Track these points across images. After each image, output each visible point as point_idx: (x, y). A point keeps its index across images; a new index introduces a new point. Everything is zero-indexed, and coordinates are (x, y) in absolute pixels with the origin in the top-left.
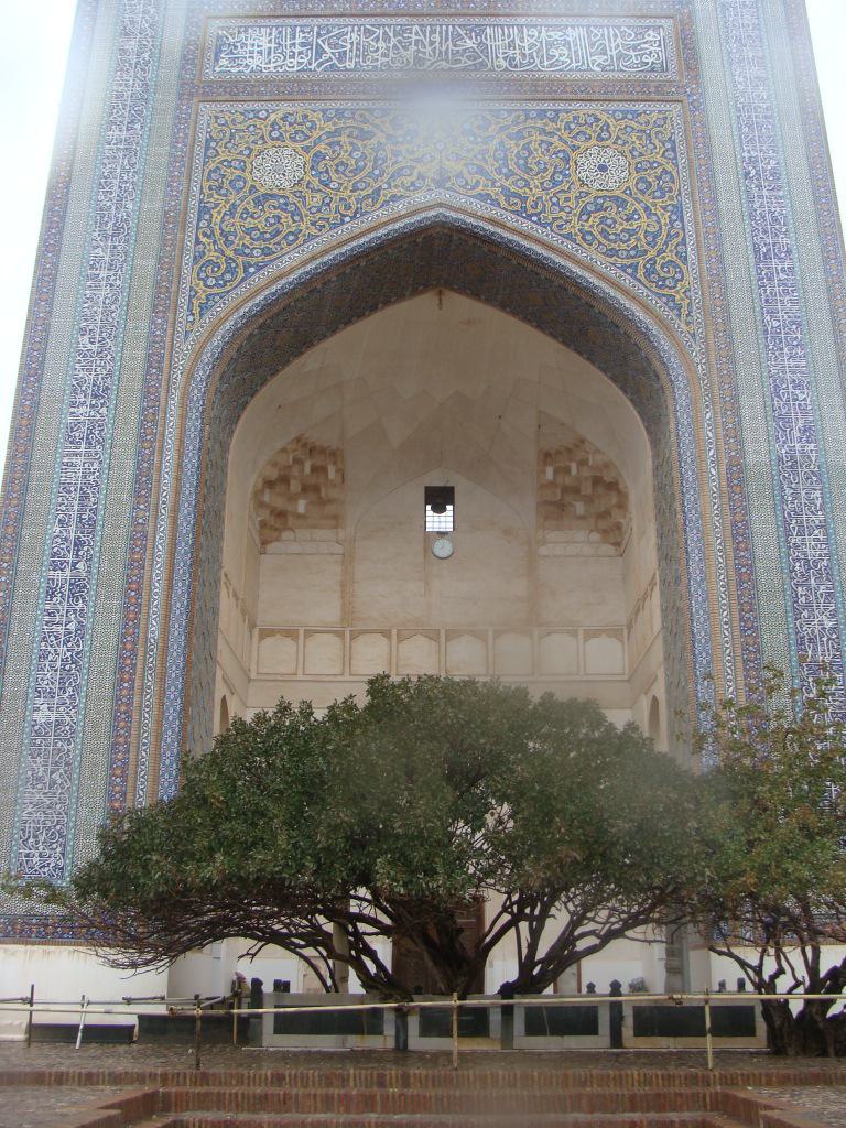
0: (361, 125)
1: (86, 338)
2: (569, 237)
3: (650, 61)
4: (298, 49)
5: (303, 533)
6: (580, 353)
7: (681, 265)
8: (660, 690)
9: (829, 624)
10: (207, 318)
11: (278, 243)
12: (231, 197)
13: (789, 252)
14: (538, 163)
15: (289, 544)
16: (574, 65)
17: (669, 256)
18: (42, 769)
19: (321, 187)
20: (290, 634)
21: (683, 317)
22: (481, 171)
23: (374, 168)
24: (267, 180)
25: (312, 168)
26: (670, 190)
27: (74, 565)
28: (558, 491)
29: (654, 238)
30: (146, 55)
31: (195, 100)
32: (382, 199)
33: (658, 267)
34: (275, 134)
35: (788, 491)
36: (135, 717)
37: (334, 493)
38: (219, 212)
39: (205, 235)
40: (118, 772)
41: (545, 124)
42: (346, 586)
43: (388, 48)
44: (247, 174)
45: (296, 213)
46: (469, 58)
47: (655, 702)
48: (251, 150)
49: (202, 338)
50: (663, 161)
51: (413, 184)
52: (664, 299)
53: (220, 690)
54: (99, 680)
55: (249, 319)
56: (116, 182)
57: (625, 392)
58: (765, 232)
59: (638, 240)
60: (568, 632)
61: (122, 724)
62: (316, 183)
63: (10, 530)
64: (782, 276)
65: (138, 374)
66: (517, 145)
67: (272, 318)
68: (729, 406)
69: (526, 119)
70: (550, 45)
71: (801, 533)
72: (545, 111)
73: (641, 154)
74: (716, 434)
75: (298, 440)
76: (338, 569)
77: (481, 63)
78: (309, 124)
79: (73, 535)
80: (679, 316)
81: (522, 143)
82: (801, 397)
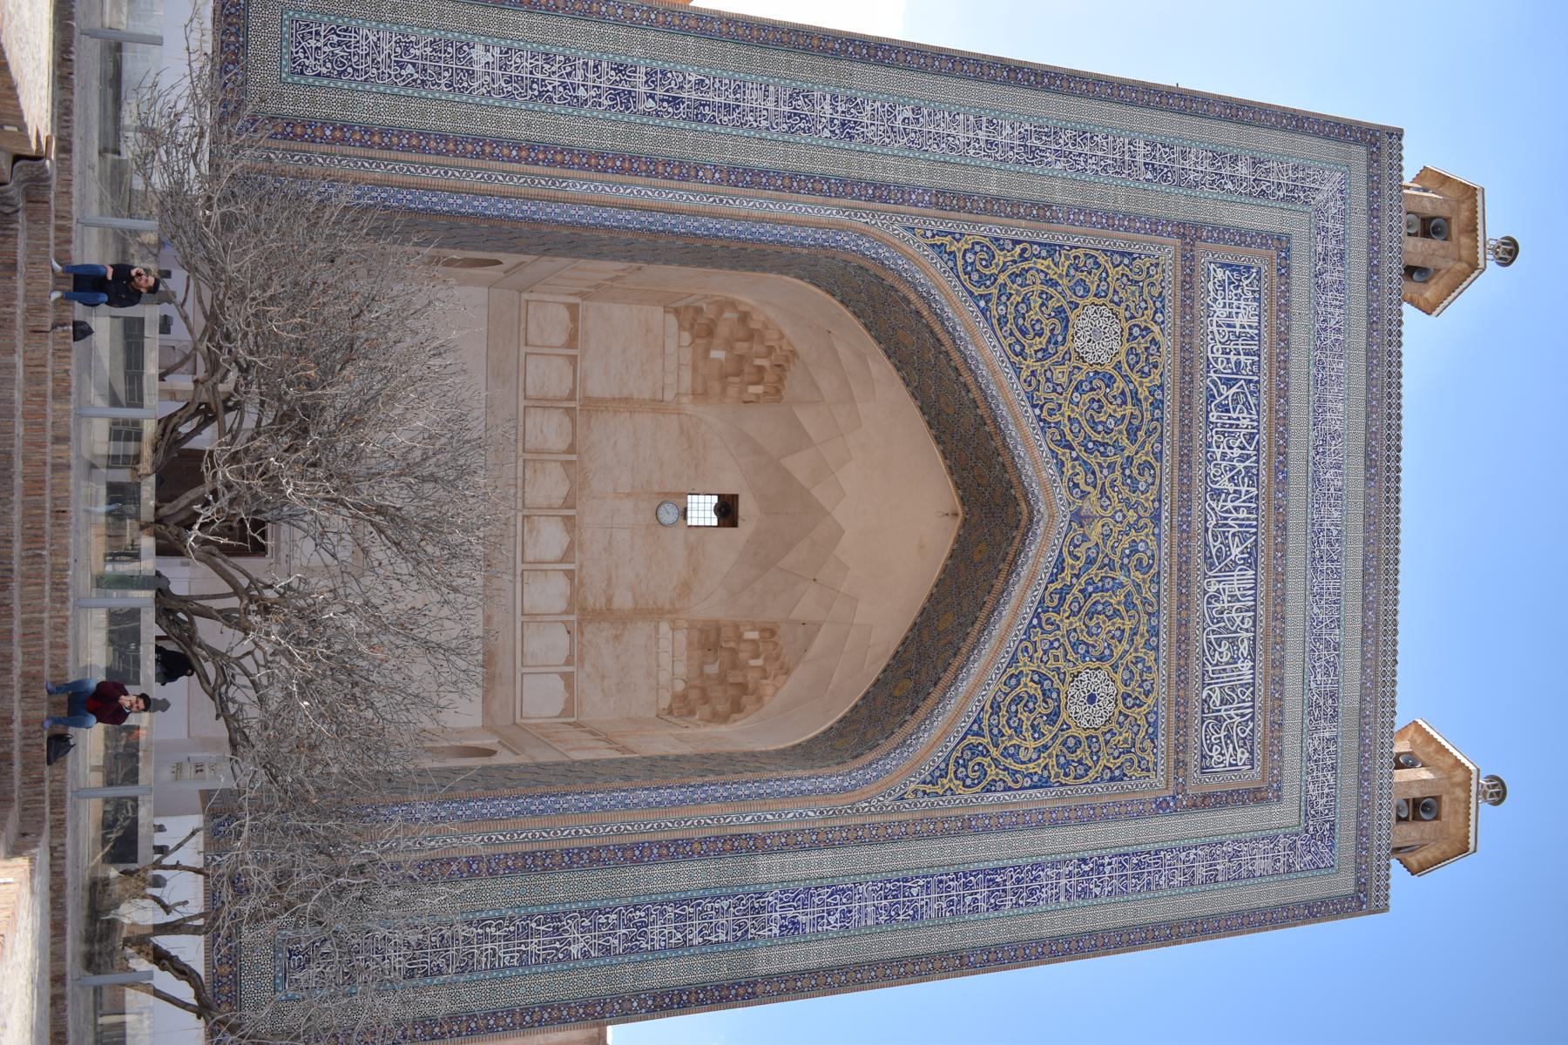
0: (1144, 428)
1: (910, 114)
2: (1014, 660)
3: (1214, 754)
4: (1233, 358)
5: (687, 356)
6: (885, 671)
7: (984, 783)
8: (504, 758)
9: (574, 949)
10: (929, 252)
11: (1012, 334)
12: (1065, 281)
13: (996, 907)
14: (1098, 626)
15: (677, 340)
16: (1210, 668)
17: (992, 772)
18: (418, 53)
19: (1074, 383)
20: (572, 341)
21: (922, 787)
22: (1090, 562)
23: (1095, 442)
24: (1082, 322)
25: (1096, 373)
26: (1066, 775)
27: (652, 96)
28: (732, 645)
29: (1011, 756)
30: (1230, 186)
31: (1178, 242)
32: (1060, 451)
33: (979, 759)
34: (1136, 331)
35: (725, 904)
36: (477, 163)
37: (732, 391)
38: (1048, 267)
39: (1024, 250)
40: (414, 142)
41: (1142, 635)
42: (626, 403)
43: (1231, 460)
44: (1091, 299)
46: (1220, 550)
47: (489, 753)
48: (1118, 304)
49: (902, 244)
50: (1099, 767)
51: (1076, 485)
52: (943, 766)
53: (509, 259)
54: (521, 122)
55: (927, 300)
56: (1086, 150)
57: (840, 721)
58: (1018, 881)
59: (1011, 738)
60: (571, 655)
61: (470, 147)
62: (1079, 376)
63: (693, 23)
64: (968, 900)
65: (867, 174)
66: (1119, 603)
67: (927, 326)
68: (822, 837)
69: (1149, 614)
70: (1233, 642)
71: (678, 917)
72: (1157, 635)
73: (1107, 742)
74: (790, 821)
75: (794, 353)
76: (647, 396)
77: (1212, 564)
78: (1146, 369)
79: (686, 95)
80: (924, 782)
81: (1122, 608)
82: (832, 919)
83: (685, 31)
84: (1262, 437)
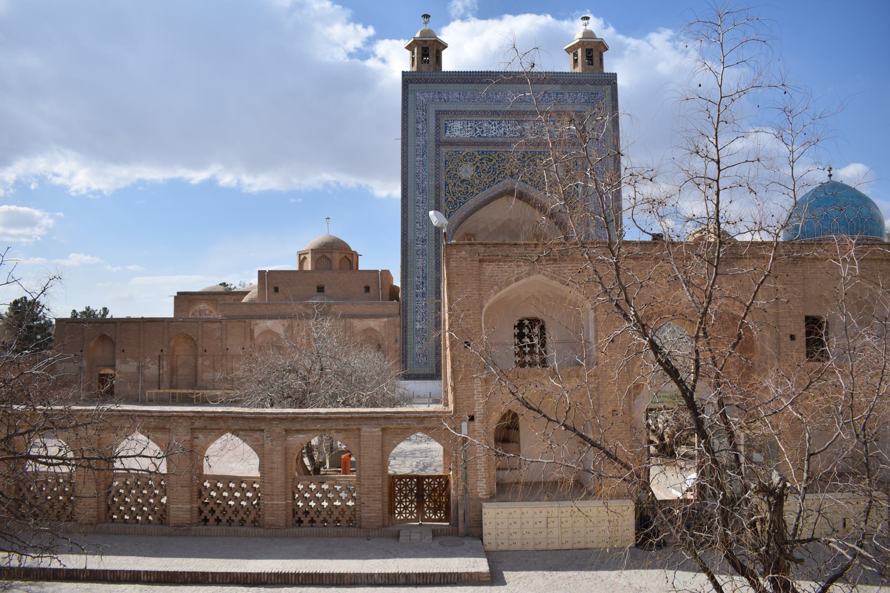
45: (472, 186)
65: (434, 235)
83: (407, 281)
84: (490, 119)
